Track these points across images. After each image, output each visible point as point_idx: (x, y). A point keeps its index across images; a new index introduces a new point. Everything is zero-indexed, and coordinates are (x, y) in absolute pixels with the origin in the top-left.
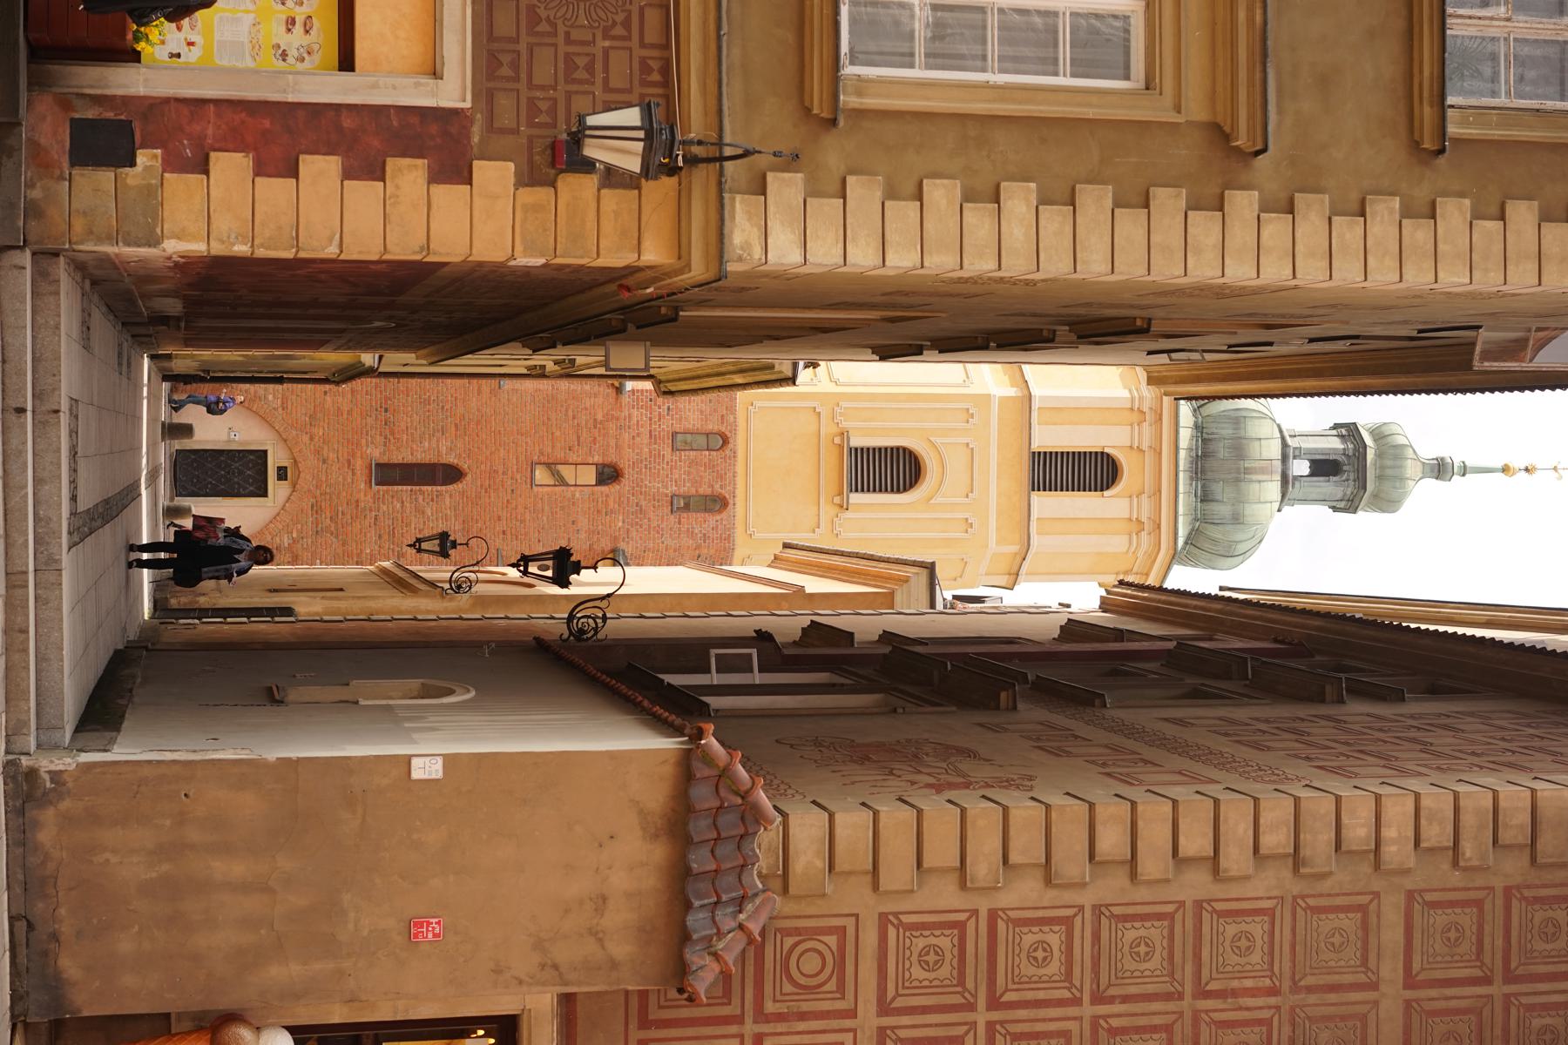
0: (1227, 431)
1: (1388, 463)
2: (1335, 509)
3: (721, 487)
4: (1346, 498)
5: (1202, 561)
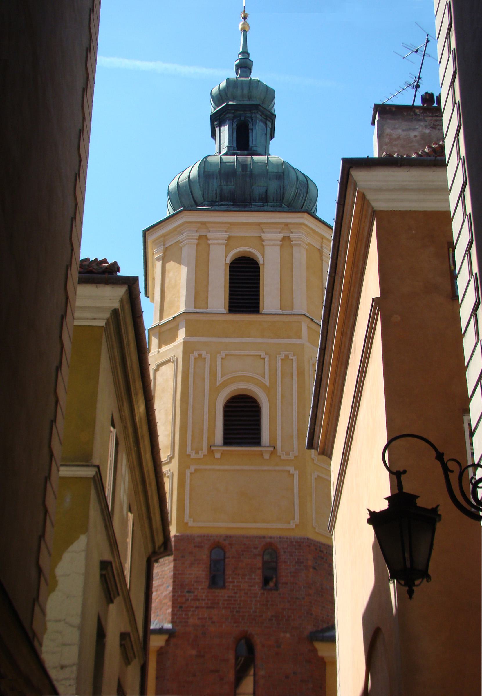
0: (215, 184)
1: (239, 91)
2: (272, 136)
3: (256, 548)
4: (264, 120)
5: (311, 207)
